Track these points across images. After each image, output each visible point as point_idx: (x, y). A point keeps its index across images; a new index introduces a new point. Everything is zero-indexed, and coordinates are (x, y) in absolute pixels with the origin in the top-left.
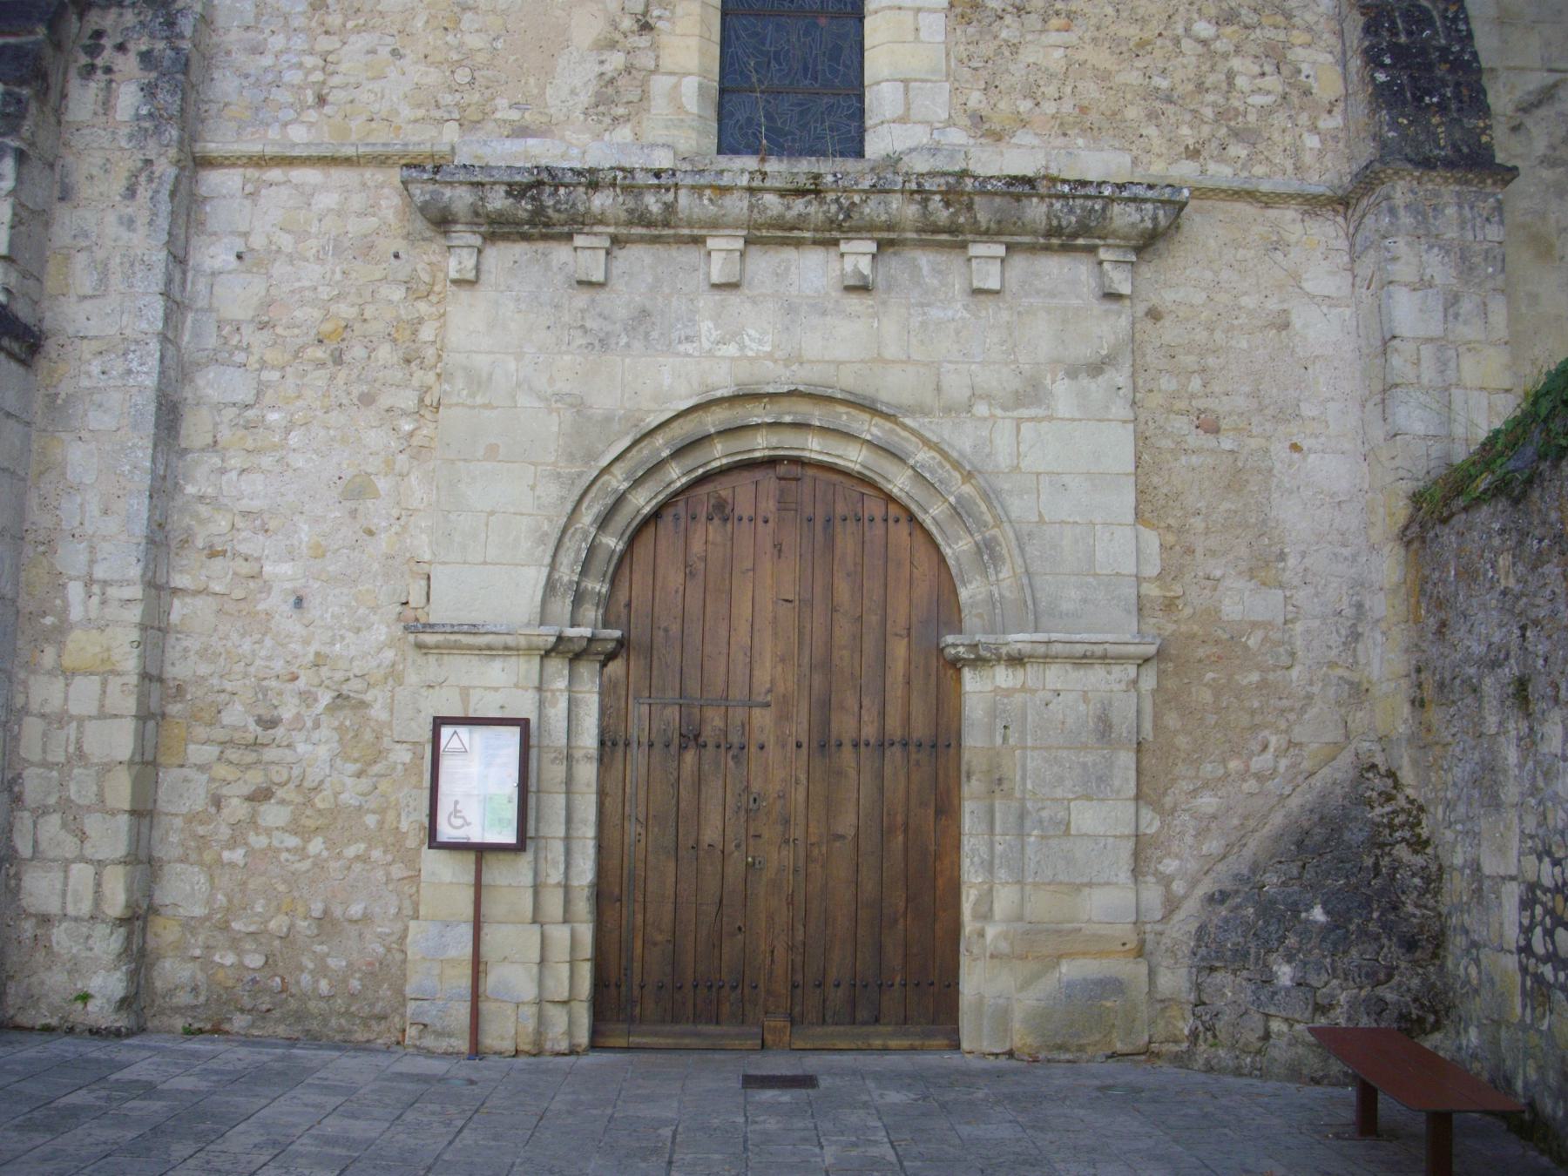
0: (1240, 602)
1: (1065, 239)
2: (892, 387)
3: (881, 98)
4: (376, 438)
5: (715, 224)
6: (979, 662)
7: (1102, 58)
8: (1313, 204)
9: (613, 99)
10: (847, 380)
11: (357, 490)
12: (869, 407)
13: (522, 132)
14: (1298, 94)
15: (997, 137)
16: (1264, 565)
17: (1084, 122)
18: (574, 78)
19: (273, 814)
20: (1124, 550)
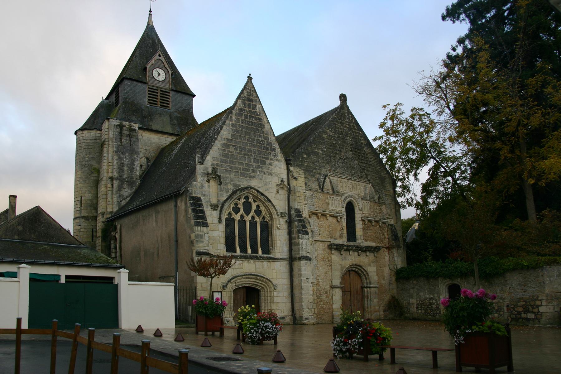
0: (383, 282)
1: (373, 252)
2: (362, 264)
3: (358, 237)
4: (327, 268)
5: (351, 250)
6: (367, 287)
7: (373, 234)
8: (386, 248)
9: (341, 236)
10: (358, 263)
11: (326, 273)
12: (360, 266)
13: (335, 239)
14: (385, 238)
15: (366, 241)
16: (384, 279)
17: (372, 240)
18: (338, 234)
19: (322, 303)
20: (376, 278)
